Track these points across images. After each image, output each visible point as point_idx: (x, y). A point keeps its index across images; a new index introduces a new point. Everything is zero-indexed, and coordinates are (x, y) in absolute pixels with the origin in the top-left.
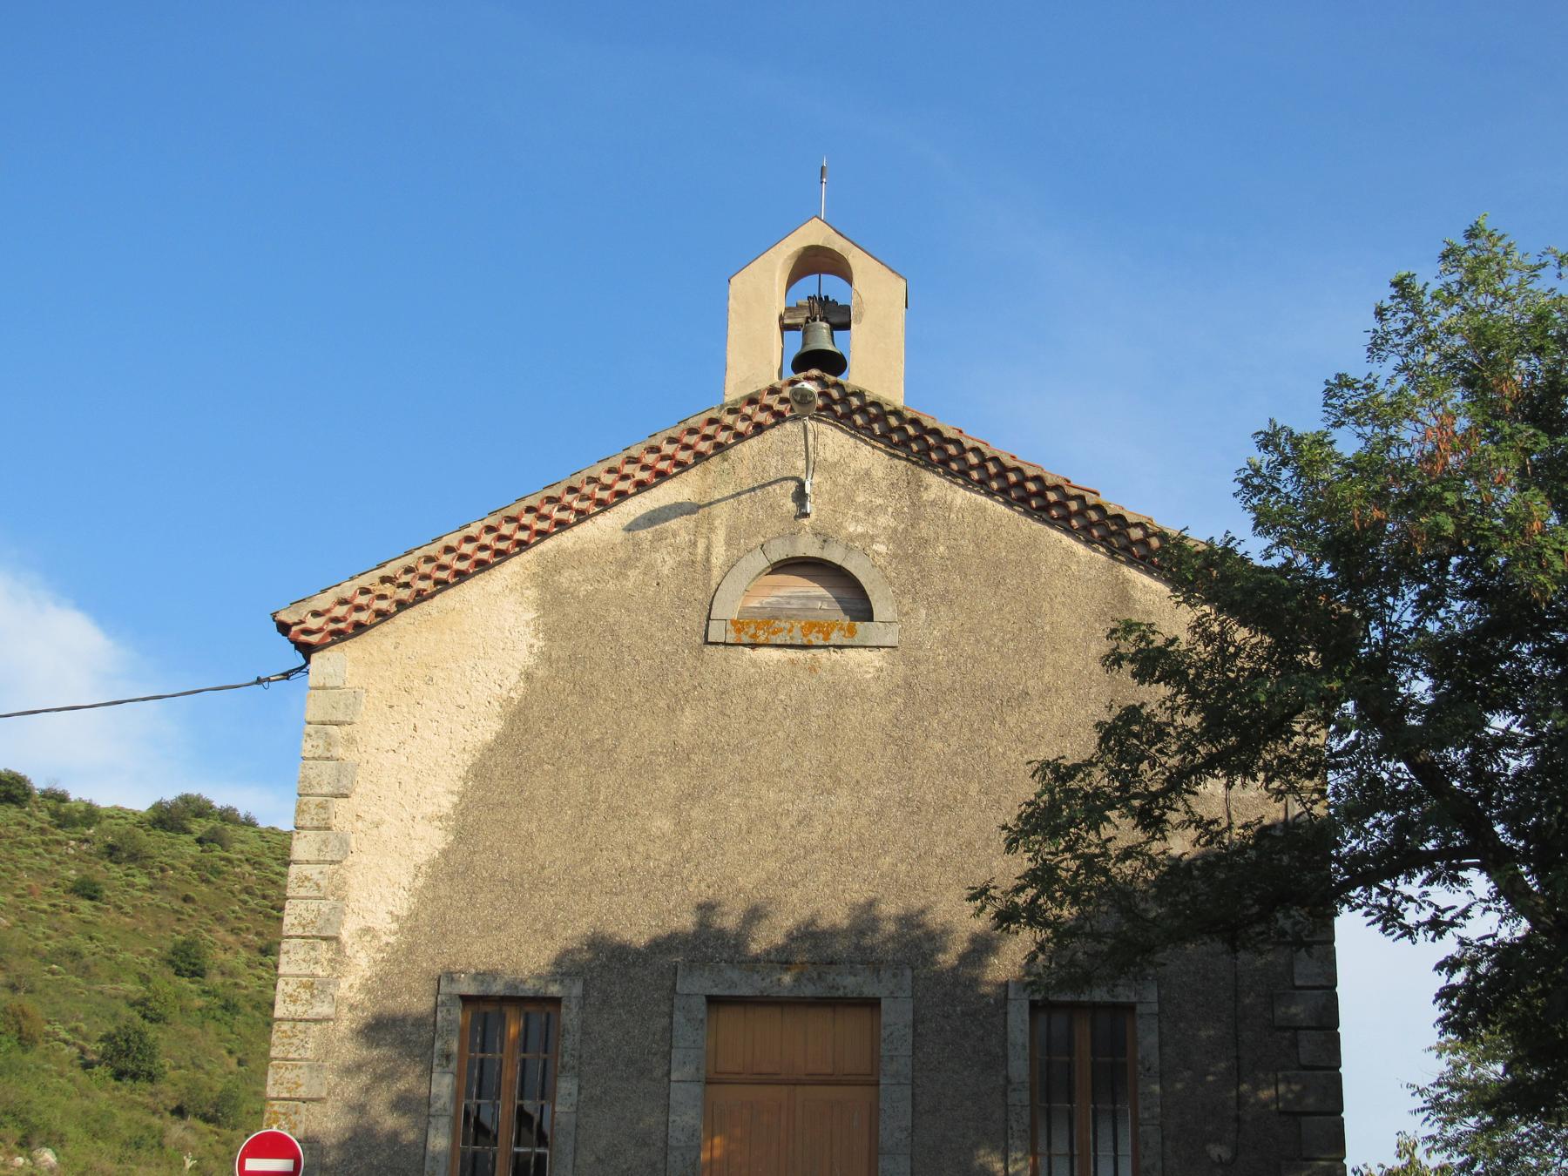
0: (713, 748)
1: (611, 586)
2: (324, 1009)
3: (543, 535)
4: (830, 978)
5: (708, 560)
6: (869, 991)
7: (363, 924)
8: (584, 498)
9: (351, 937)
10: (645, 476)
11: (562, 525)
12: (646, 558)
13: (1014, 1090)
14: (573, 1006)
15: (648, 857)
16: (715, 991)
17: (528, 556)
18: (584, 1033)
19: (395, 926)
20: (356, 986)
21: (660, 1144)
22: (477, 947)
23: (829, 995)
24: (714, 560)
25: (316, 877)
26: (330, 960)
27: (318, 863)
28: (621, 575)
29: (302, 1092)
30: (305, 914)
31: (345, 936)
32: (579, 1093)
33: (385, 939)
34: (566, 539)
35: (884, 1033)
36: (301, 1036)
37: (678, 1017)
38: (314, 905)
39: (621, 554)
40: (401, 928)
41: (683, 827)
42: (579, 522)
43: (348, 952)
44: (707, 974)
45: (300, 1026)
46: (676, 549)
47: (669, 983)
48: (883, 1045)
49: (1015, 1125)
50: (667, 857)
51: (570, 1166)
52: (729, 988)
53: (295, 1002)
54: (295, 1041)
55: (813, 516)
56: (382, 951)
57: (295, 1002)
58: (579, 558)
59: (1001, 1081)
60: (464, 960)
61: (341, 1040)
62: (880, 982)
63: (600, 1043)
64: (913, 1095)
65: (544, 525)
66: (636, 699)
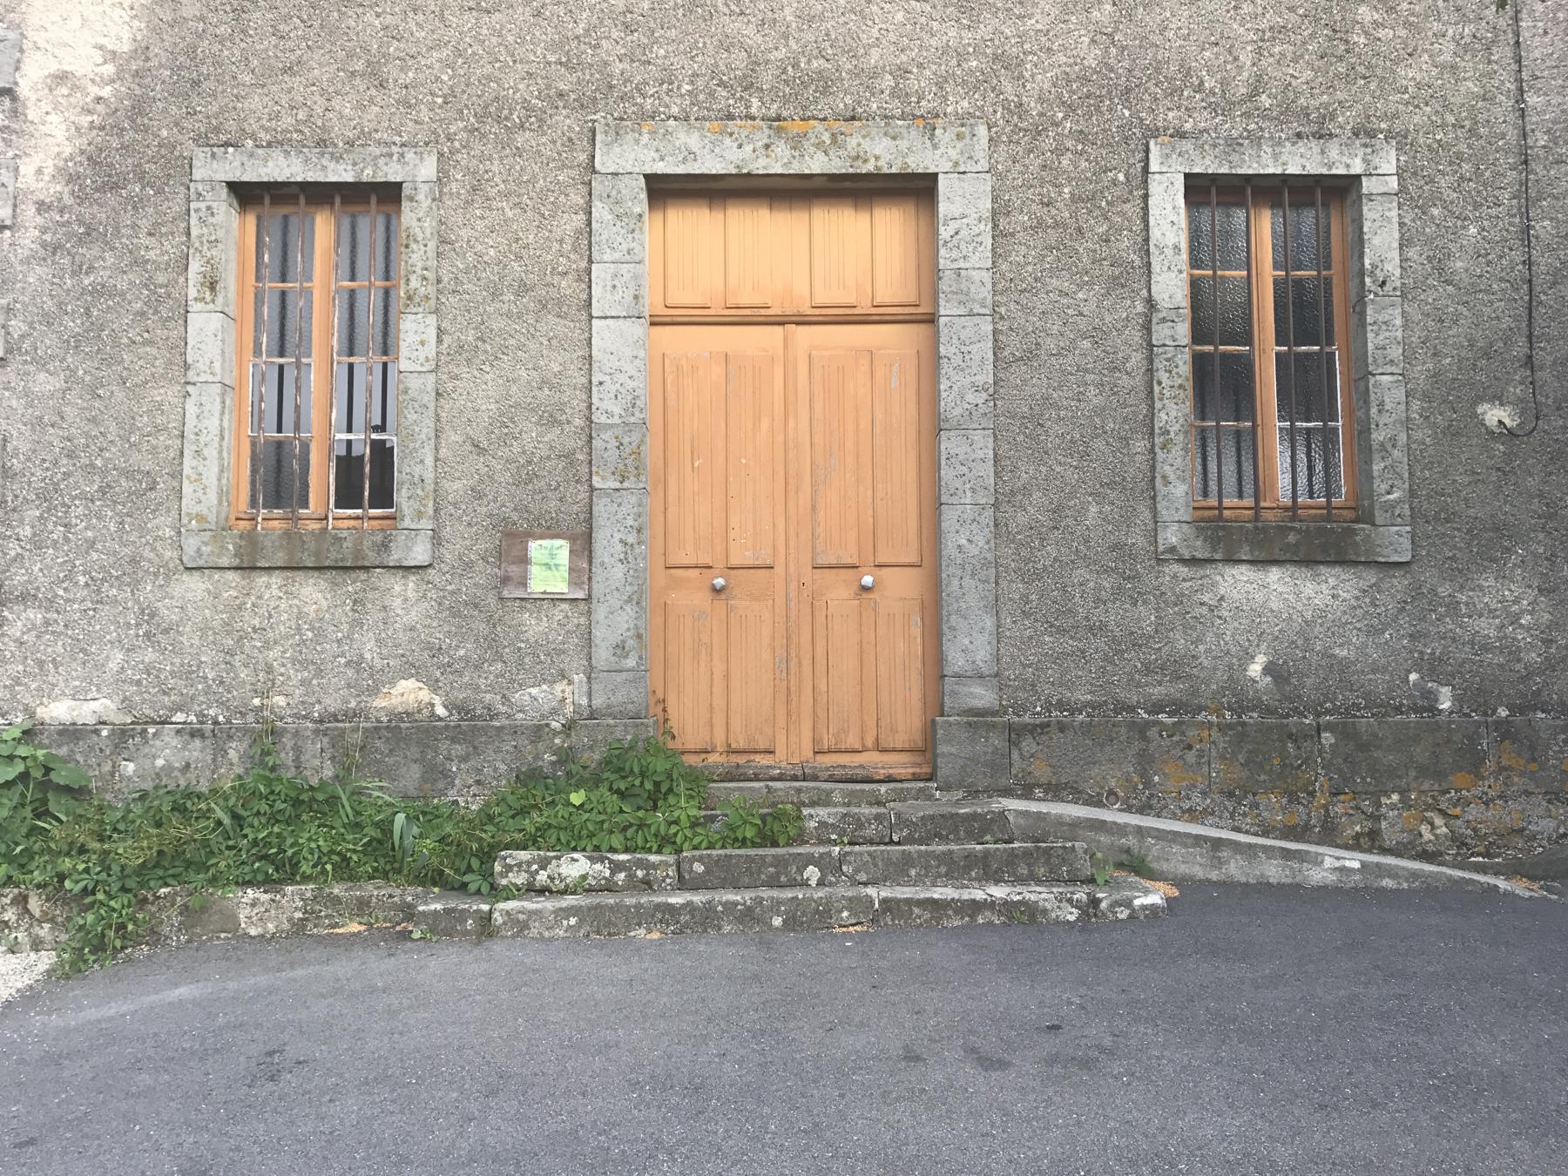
4: (852, 142)
6: (920, 160)
7: (54, 67)
9: (34, 88)
13: (1164, 320)
14: (421, 197)
16: (661, 168)
18: (443, 241)
19: (109, 69)
20: (49, 171)
21: (578, 422)
22: (255, 102)
23: (851, 171)
31: (24, 90)
32: (440, 341)
33: (95, 91)
35: (945, 233)
37: (600, 210)
40: (119, 77)
43: (32, 114)
44: (645, 138)
47: (583, 157)
48: (942, 252)
51: (429, 461)
52: (685, 160)
56: (90, 112)
59: (1140, 307)
61: (26, 261)
62: (935, 147)
63: (470, 257)
64: (995, 332)
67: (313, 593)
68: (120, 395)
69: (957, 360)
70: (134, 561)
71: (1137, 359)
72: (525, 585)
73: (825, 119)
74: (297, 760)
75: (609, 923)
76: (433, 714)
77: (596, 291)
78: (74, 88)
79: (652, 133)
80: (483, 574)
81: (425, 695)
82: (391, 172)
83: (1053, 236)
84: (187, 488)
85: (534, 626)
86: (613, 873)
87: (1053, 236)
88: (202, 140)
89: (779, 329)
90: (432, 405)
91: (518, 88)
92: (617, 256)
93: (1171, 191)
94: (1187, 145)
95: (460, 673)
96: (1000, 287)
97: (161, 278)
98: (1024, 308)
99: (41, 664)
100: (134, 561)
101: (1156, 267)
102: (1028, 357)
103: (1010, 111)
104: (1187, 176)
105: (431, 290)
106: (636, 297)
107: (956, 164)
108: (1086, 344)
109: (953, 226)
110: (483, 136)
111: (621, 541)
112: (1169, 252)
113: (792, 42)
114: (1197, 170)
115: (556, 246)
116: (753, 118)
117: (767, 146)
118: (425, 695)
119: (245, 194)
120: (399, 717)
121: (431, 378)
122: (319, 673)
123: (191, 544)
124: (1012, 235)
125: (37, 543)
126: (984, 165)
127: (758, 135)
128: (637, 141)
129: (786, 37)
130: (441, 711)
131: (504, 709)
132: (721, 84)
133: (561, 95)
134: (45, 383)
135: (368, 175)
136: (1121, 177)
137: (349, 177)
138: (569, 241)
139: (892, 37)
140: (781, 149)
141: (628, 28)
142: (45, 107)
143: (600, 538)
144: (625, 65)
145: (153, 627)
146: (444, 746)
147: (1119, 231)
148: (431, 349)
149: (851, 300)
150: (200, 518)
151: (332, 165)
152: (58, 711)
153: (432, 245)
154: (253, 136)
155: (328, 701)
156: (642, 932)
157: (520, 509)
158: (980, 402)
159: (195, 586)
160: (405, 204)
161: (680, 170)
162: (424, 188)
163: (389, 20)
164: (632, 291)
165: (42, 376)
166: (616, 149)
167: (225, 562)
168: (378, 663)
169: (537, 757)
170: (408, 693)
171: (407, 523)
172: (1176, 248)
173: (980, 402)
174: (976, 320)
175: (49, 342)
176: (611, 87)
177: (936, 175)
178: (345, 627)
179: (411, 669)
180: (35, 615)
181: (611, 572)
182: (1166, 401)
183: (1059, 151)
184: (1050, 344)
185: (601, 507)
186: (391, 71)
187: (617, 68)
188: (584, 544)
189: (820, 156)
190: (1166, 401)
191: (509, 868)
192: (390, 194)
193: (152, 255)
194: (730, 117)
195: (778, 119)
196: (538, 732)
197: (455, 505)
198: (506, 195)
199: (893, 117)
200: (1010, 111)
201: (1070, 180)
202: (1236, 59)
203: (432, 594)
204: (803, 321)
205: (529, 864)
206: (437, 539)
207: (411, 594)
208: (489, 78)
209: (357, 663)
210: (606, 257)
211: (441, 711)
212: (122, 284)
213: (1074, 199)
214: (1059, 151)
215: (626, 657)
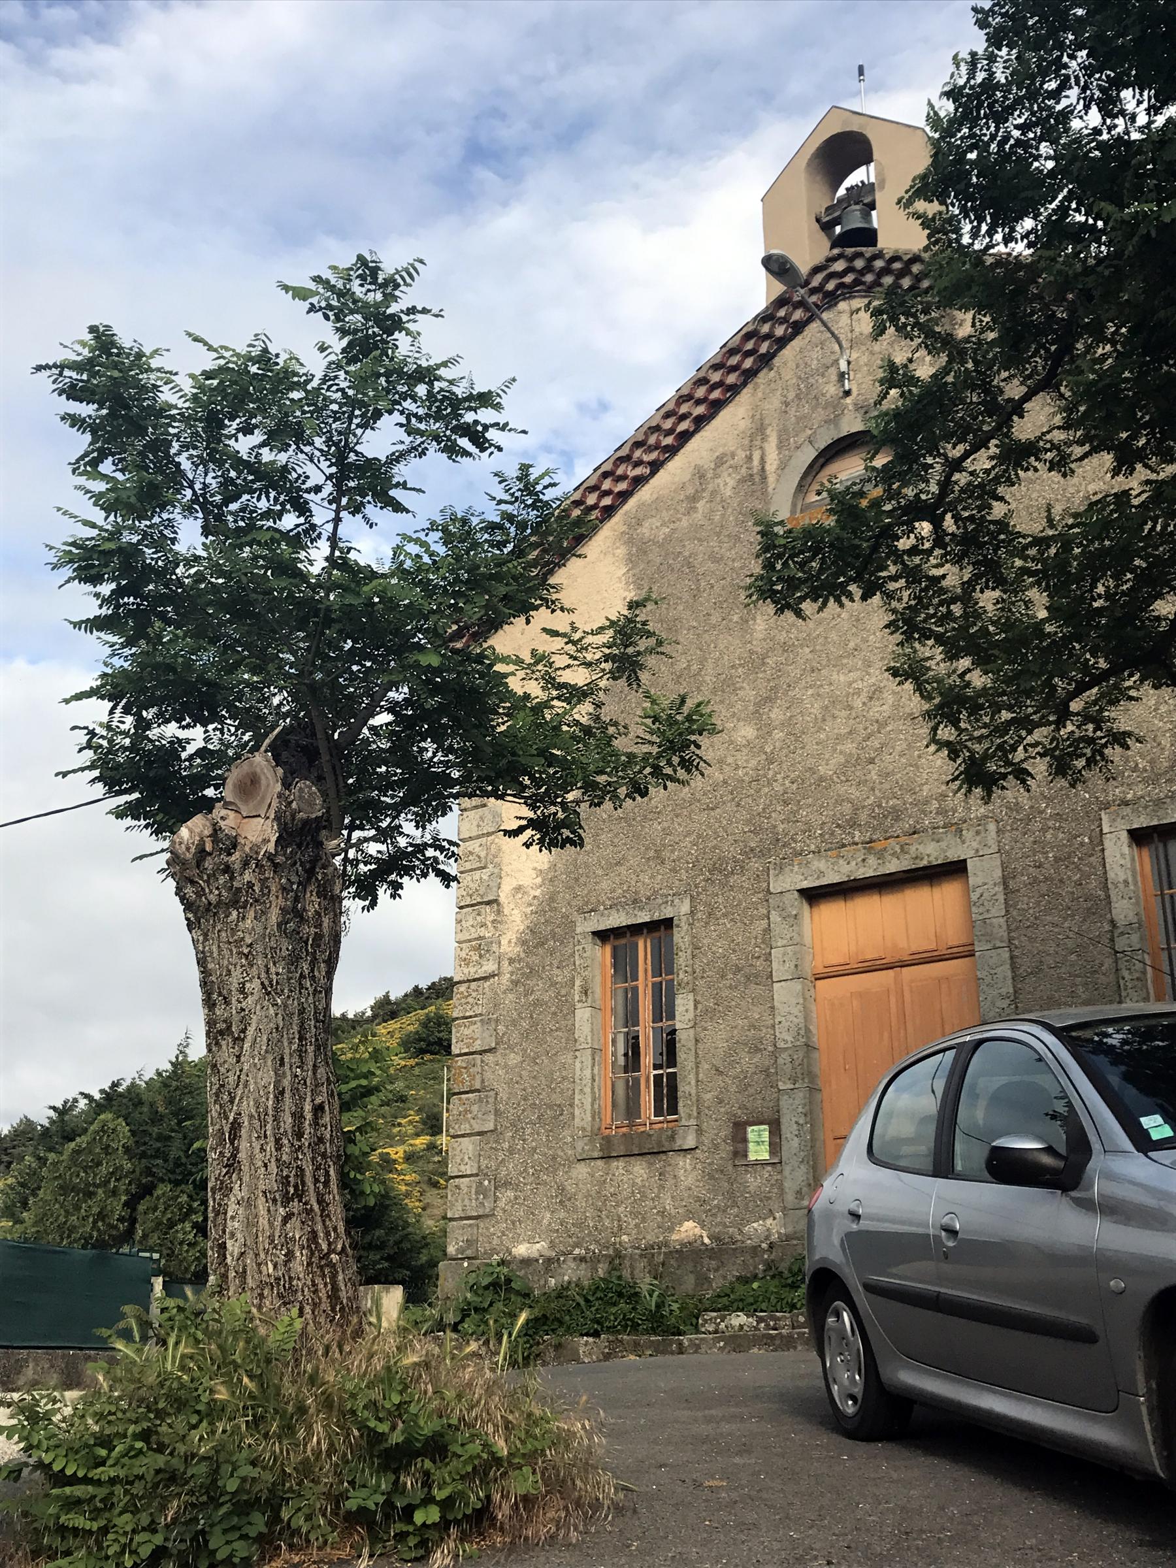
0: (786, 648)
1: (685, 523)
2: (489, 967)
3: (624, 496)
4: (913, 849)
5: (763, 469)
6: (953, 855)
7: (515, 884)
8: (650, 449)
9: (507, 897)
10: (700, 410)
11: (639, 481)
12: (710, 487)
13: (1122, 934)
14: (683, 924)
15: (737, 768)
16: (805, 884)
17: (617, 519)
19: (539, 880)
20: (514, 941)
22: (605, 885)
23: (914, 867)
24: (768, 467)
25: (477, 850)
26: (493, 922)
27: (478, 837)
28: (691, 510)
29: (477, 1046)
30: (472, 885)
31: (502, 899)
32: (696, 1008)
34: (645, 494)
35: (974, 897)
36: (474, 994)
37: (775, 917)
38: (477, 875)
39: (690, 491)
41: (765, 730)
42: (653, 473)
43: (506, 911)
44: (796, 868)
45: (474, 985)
46: (735, 468)
48: (974, 909)
49: (1126, 974)
50: (753, 763)
51: (693, 1082)
52: (818, 878)
53: (467, 965)
54: (470, 1000)
55: (855, 392)
56: (531, 905)
57: (467, 965)
58: (658, 504)
59: (1107, 927)
60: (593, 900)
61: (504, 992)
62: (963, 842)
63: (710, 955)
64: (1012, 958)
65: (622, 486)
66: (714, 620)
67: (640, 1170)
68: (546, 1061)
69: (988, 980)
70: (554, 1158)
71: (1108, 963)
72: (746, 1156)
73: (898, 837)
74: (632, 1273)
75: (739, 1345)
76: (703, 1244)
77: (775, 965)
78: (525, 893)
79: (799, 864)
80: (726, 1149)
81: (698, 1231)
82: (668, 913)
83: (1044, 888)
84: (577, 1112)
85: (753, 1181)
86: (758, 1323)
87: (1044, 888)
88: (581, 911)
89: (890, 971)
90: (693, 1049)
91: (732, 851)
92: (785, 942)
93: (1119, 843)
94: (1127, 810)
95: (714, 1215)
96: (1013, 927)
97: (563, 992)
98: (1030, 938)
99: (513, 1223)
100: (554, 1158)
101: (1113, 898)
102: (1037, 971)
103: (1011, 809)
104: (1129, 831)
105: (690, 978)
106: (796, 966)
107: (977, 851)
108: (1073, 957)
109: (979, 891)
110: (713, 882)
111: (796, 1122)
112: (1121, 886)
113: (877, 792)
114: (1135, 826)
115: (753, 941)
116: (857, 844)
117: (864, 860)
118: (698, 1231)
119: (602, 936)
120: (683, 1245)
121: (692, 1031)
122: (644, 1220)
123: (580, 1145)
124: (1018, 891)
125: (511, 1151)
126: (995, 848)
127: (858, 854)
128: (792, 871)
129: (873, 789)
130: (707, 1241)
131: (739, 1238)
132: (838, 826)
133: (752, 850)
134: (514, 1059)
135: (656, 916)
136: (1086, 840)
137: (647, 919)
138: (760, 936)
139: (935, 776)
140: (872, 861)
141: (786, 803)
142: (512, 906)
143: (784, 1121)
144: (785, 825)
145: (564, 1198)
146: (706, 1261)
147: (1089, 877)
148: (691, 1015)
149: (933, 947)
150: (584, 1129)
151: (639, 913)
152: (522, 1250)
153: (689, 951)
154: (603, 904)
155: (649, 1237)
156: (755, 1350)
157: (743, 1107)
158: (1005, 1006)
159: (582, 1170)
160: (675, 930)
161: (817, 884)
162: (684, 919)
163: (665, 825)
164: (794, 963)
165: (512, 1055)
166: (781, 877)
167: (596, 1154)
168: (673, 1212)
169: (756, 1267)
170: (689, 1229)
171: (684, 1122)
172: (1126, 882)
173: (1005, 1006)
174: (999, 951)
175: (515, 1037)
176: (778, 840)
177: (965, 860)
178: (656, 1190)
179: (690, 1215)
180: (510, 1194)
181: (792, 1144)
182: (1130, 991)
183: (1044, 830)
184: (1050, 961)
185: (785, 1102)
186: (666, 854)
187: (781, 828)
188: (775, 1128)
189: (895, 860)
190: (1130, 991)
191: (706, 1321)
192: (668, 923)
193: (559, 979)
194: (844, 846)
195: (870, 842)
196: (755, 1250)
197: (708, 1108)
198: (725, 915)
199: (938, 828)
200: (1011, 809)
201: (1052, 848)
202: (1159, 744)
203: (699, 1166)
204: (903, 965)
205: (716, 1318)
206: (700, 1131)
207: (688, 1167)
208: (715, 847)
209: (662, 1213)
210: (779, 944)
211: (707, 1241)
212: (546, 999)
213: (1056, 858)
214: (1044, 830)
215: (803, 1199)
